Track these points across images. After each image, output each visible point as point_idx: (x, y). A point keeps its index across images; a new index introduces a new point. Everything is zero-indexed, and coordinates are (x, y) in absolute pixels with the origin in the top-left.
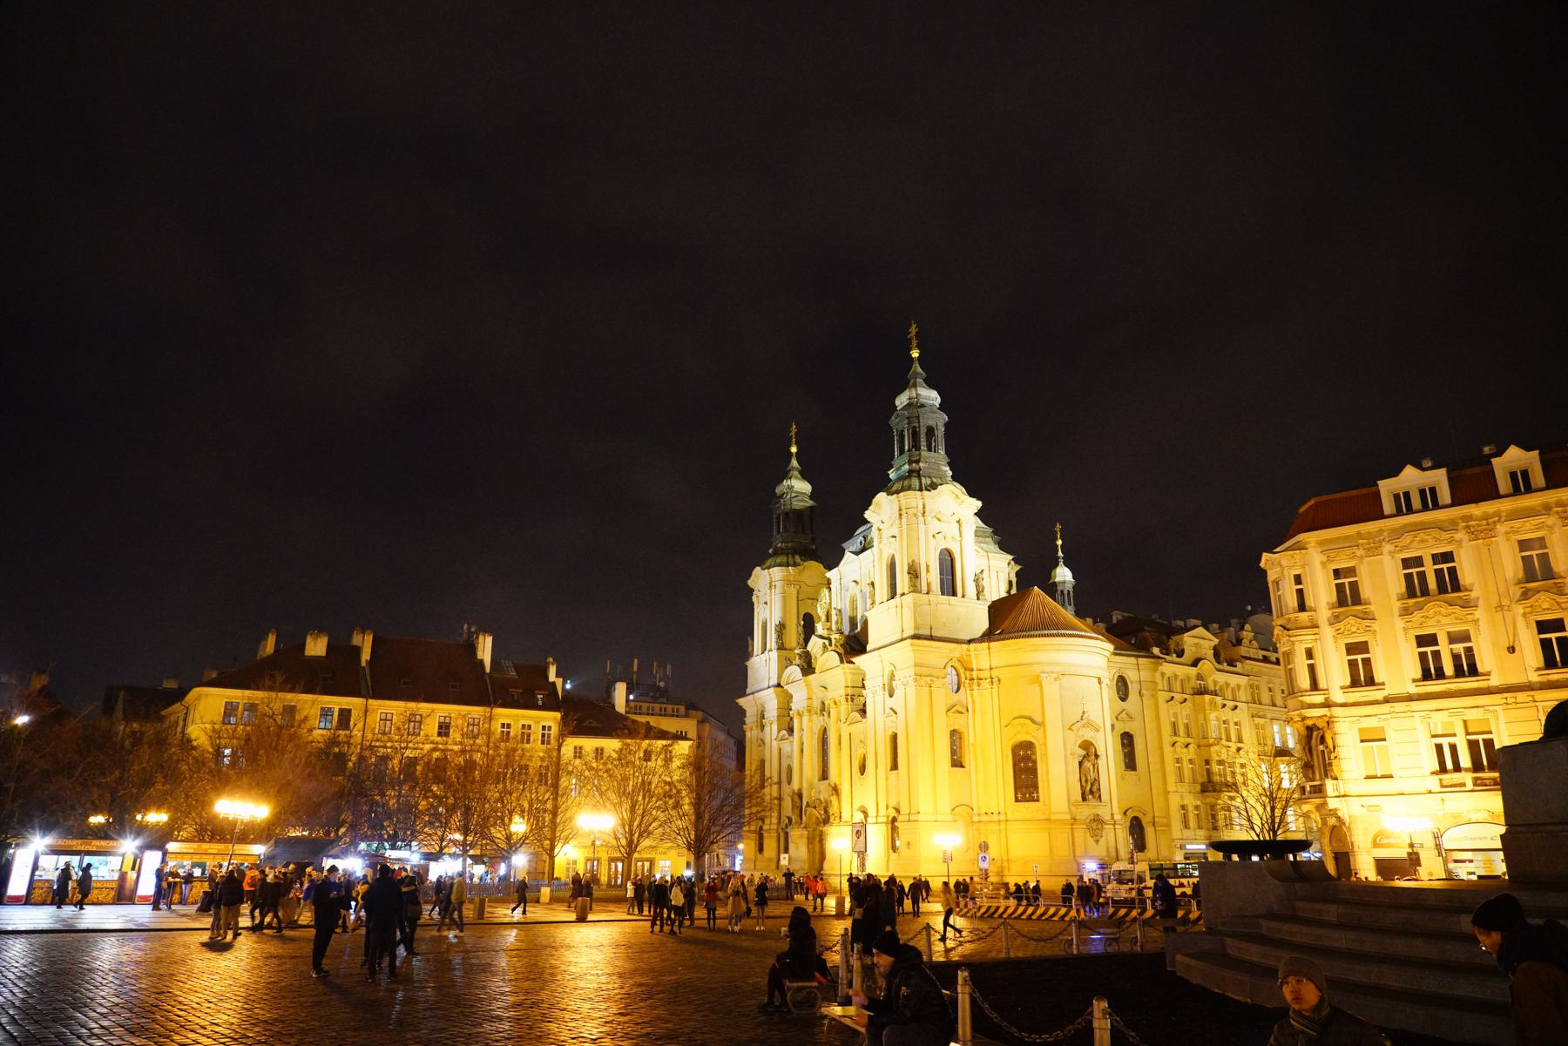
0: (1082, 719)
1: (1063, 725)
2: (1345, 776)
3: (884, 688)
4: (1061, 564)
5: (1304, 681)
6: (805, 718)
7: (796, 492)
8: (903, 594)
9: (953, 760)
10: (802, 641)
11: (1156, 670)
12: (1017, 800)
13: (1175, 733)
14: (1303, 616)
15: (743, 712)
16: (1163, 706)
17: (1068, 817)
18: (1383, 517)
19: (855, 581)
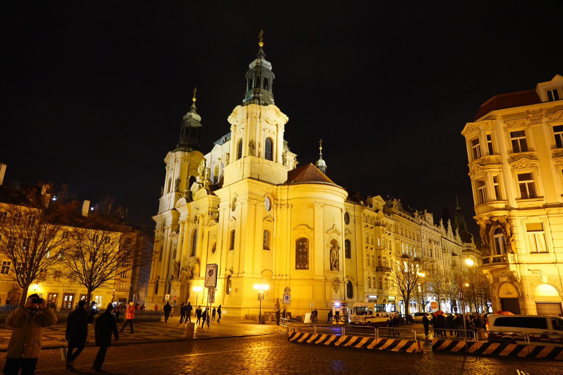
0: (333, 228)
1: (324, 230)
2: (519, 251)
3: (230, 206)
4: (321, 158)
5: (492, 195)
6: (186, 225)
8: (245, 157)
9: (264, 246)
10: (188, 186)
11: (361, 211)
12: (296, 268)
13: (368, 242)
14: (493, 157)
15: (155, 223)
16: (363, 229)
17: (323, 278)
18: (541, 102)
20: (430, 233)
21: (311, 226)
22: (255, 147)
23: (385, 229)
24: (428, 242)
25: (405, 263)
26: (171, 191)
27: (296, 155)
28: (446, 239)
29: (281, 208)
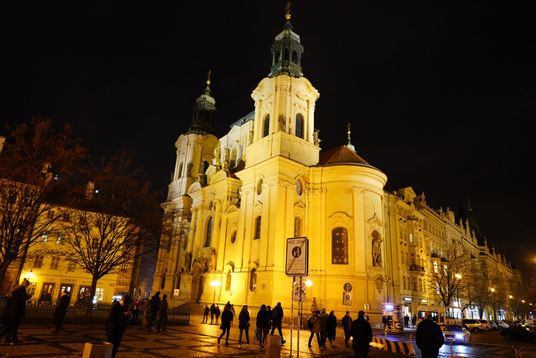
0: (374, 217)
1: (364, 219)
3: (255, 189)
4: (349, 143)
6: (199, 212)
7: (207, 101)
8: (273, 133)
10: (202, 170)
13: (401, 237)
17: (365, 275)
21: (350, 214)
24: (451, 242)
25: (435, 263)
26: (182, 176)
28: (466, 240)
29: (314, 192)
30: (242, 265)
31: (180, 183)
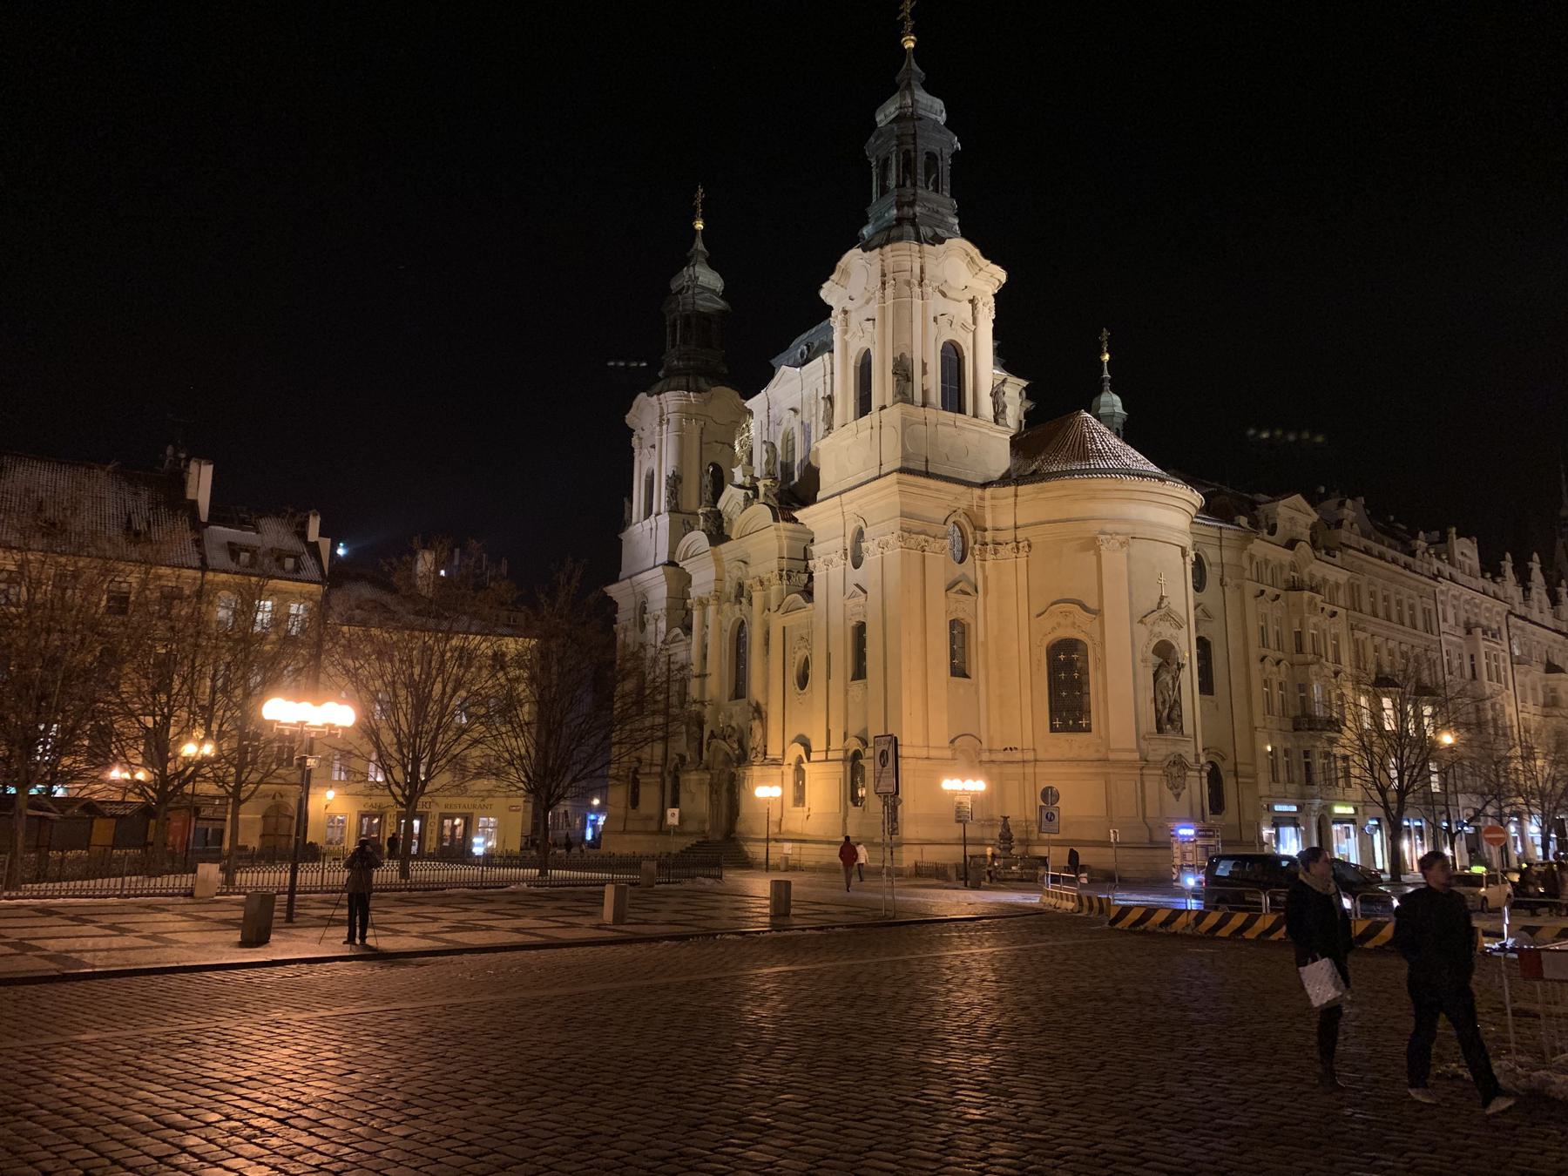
0: (1159, 607)
3: (846, 555)
4: (1107, 385)
6: (711, 609)
7: (703, 287)
8: (883, 407)
9: (952, 665)
10: (708, 496)
11: (1242, 548)
12: (1053, 729)
13: (1264, 643)
15: (612, 605)
16: (1249, 599)
17: (1136, 756)
19: (792, 409)
20: (1467, 602)
21: (1092, 603)
22: (910, 375)
23: (1319, 598)
24: (1461, 632)
25: (1387, 703)
26: (655, 510)
27: (1024, 383)
28: (1524, 618)
30: (828, 743)
31: (651, 529)
